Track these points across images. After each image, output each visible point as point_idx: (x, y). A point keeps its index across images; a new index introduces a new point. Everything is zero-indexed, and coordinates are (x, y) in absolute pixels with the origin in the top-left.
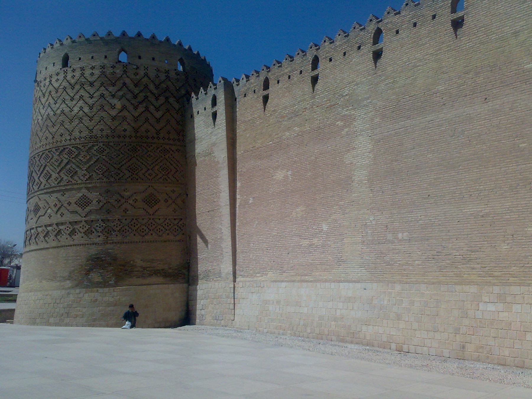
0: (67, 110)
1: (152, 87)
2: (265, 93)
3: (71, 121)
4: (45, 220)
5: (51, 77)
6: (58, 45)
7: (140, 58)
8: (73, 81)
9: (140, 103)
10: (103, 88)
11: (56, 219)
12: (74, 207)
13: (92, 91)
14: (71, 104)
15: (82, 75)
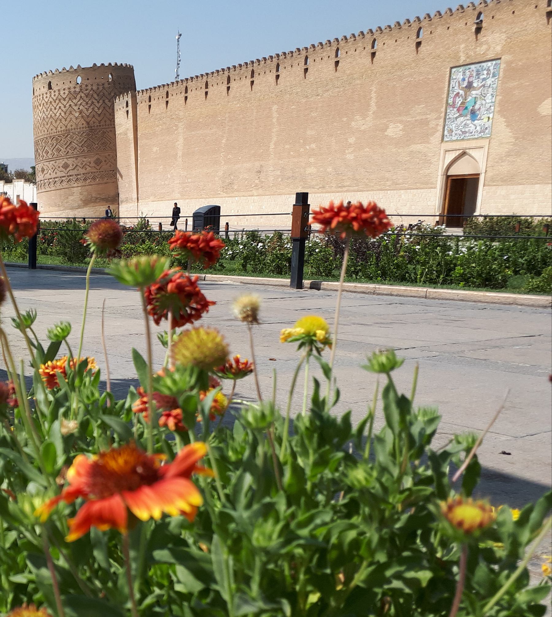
0: (53, 115)
1: (95, 96)
2: (150, 104)
3: (56, 121)
4: (48, 176)
5: (43, 95)
6: (45, 75)
7: (88, 79)
8: (55, 98)
9: (89, 107)
10: (70, 101)
11: (54, 175)
12: (61, 169)
13: (65, 103)
14: (55, 111)
15: (59, 94)
